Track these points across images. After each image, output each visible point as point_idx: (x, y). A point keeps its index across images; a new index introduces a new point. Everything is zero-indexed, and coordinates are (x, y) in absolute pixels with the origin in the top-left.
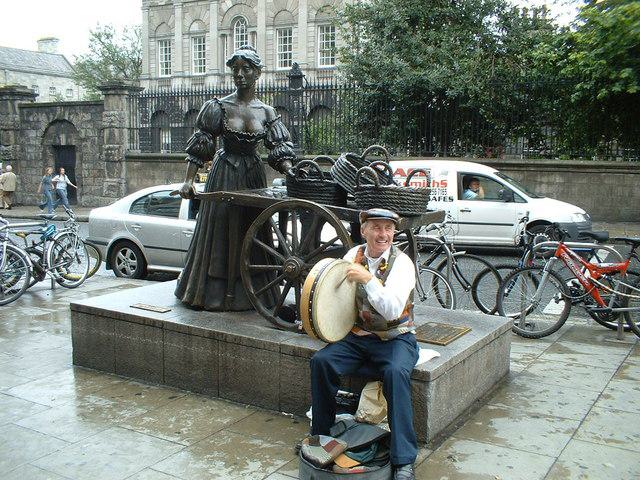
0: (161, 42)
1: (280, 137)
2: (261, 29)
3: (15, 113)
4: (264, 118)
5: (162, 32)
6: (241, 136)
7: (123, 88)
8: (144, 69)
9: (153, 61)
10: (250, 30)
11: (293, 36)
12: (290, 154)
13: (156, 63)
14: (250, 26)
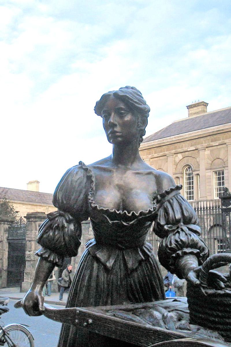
1: (178, 216)
2: (202, 171)
3: (36, 230)
4: (153, 188)
6: (113, 216)
10: (195, 173)
11: (225, 175)
12: (194, 245)
14: (195, 171)
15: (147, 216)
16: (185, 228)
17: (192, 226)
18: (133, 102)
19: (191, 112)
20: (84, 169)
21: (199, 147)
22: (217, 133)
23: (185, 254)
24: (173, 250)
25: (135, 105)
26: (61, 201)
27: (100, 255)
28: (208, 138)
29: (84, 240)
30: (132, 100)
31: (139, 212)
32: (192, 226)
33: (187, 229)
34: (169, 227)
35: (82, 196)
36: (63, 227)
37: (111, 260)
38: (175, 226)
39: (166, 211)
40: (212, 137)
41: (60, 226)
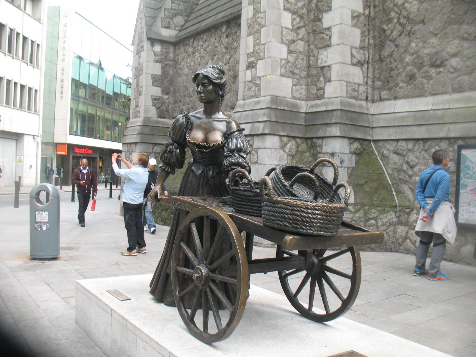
6: (199, 146)
16: (236, 155)
17: (242, 154)
24: (227, 166)
27: (193, 168)
32: (242, 154)
34: (228, 154)
35: (184, 133)
36: (173, 151)
41: (171, 151)
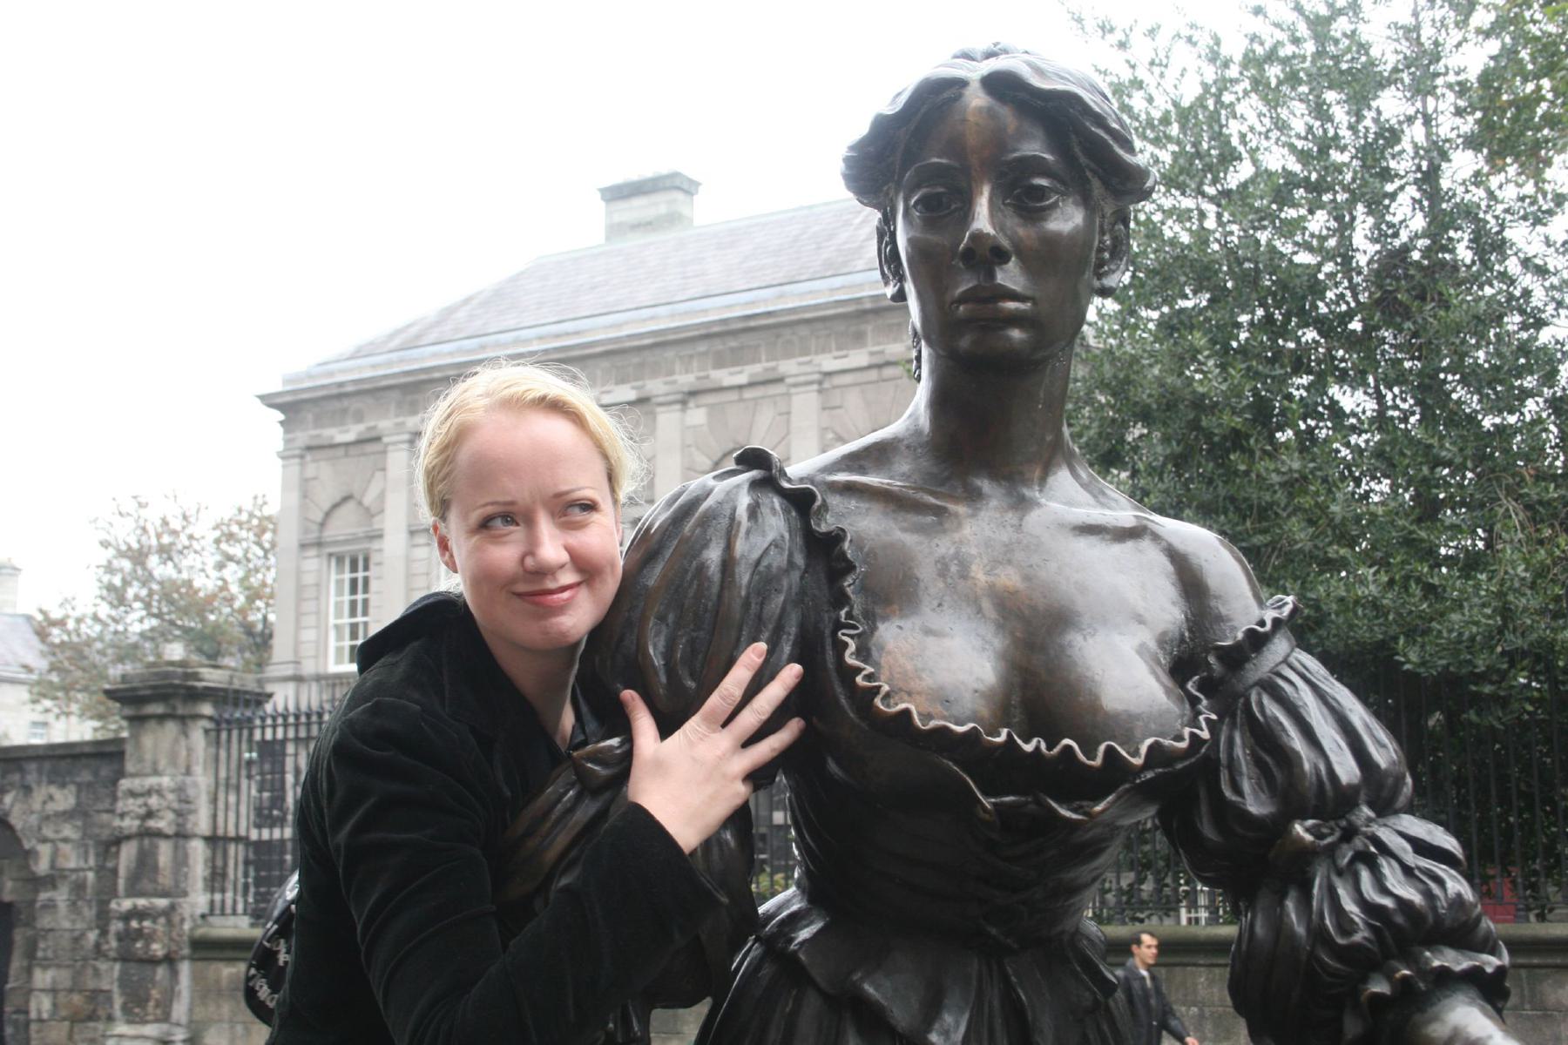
0: (340, 560)
1: (1347, 770)
4: (1169, 612)
5: (344, 525)
6: (1000, 767)
7: (196, 695)
8: (281, 649)
9: (310, 620)
13: (321, 627)
15: (1179, 766)
18: (1106, 137)
19: (617, 218)
20: (787, 495)
21: (655, 386)
22: (740, 325)
23: (1446, 980)
24: (1364, 962)
25: (1113, 151)
26: (663, 679)
28: (702, 347)
29: (91, 842)
30: (1100, 120)
31: (1144, 749)
33: (1408, 847)
37: (948, 1019)
38: (1332, 823)
39: (1266, 740)
40: (718, 345)
